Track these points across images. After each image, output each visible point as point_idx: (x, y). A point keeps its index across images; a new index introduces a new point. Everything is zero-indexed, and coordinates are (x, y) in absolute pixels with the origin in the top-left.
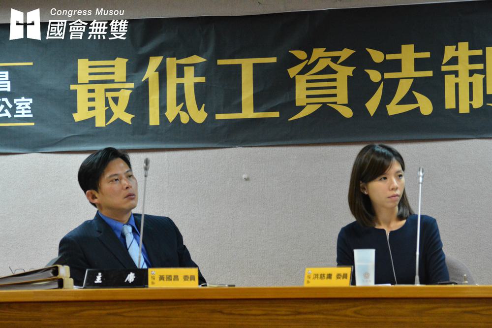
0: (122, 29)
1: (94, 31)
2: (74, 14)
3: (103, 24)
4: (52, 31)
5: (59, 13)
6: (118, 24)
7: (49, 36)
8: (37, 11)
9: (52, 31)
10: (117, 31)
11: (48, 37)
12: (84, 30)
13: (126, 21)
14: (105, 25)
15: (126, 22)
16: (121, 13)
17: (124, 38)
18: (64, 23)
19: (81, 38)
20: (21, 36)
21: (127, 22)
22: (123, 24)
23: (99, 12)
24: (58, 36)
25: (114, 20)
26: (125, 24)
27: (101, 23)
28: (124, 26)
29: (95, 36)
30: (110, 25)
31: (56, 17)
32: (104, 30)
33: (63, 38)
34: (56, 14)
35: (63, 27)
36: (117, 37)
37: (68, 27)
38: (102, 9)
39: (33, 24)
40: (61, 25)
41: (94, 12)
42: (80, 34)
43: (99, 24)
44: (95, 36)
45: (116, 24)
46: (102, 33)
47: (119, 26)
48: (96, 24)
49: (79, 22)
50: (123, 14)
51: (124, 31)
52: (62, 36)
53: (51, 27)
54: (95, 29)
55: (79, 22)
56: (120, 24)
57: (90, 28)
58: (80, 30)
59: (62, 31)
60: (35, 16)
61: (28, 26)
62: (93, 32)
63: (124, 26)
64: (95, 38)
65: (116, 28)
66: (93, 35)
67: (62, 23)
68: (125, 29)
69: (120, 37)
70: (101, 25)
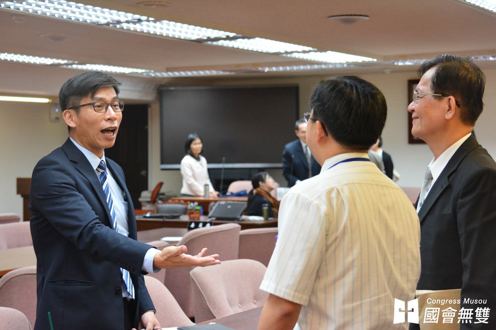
1: (463, 317)
3: (469, 311)
4: (428, 316)
5: (434, 302)
7: (426, 321)
9: (428, 316)
12: (454, 316)
14: (471, 312)
15: (488, 309)
17: (487, 323)
19: (452, 322)
23: (466, 301)
24: (433, 320)
25: (478, 308)
27: (468, 310)
32: (470, 316)
33: (437, 322)
35: (437, 313)
36: (481, 322)
37: (441, 313)
38: (469, 299)
43: (466, 311)
48: (464, 311)
49: (450, 310)
51: (486, 316)
53: (427, 313)
54: (463, 315)
57: (459, 314)
58: (451, 316)
59: (436, 317)
61: (409, 313)
64: (463, 322)
65: (480, 314)
66: (461, 320)
69: (483, 322)
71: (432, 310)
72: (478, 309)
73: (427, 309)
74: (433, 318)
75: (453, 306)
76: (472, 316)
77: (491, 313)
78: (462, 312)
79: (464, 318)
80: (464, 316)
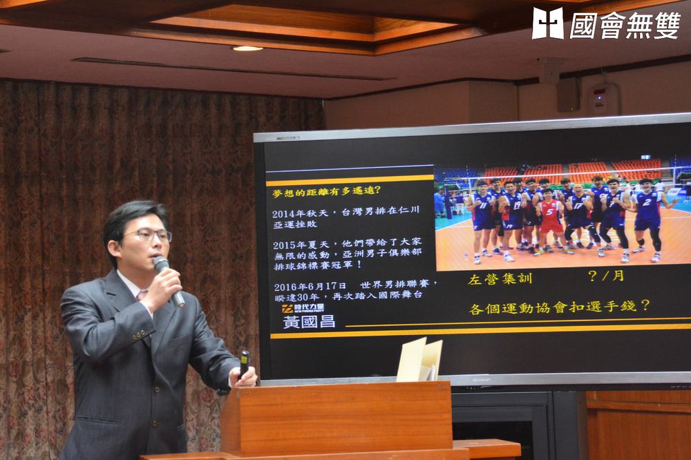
0: (672, 25)
1: (635, 28)
3: (646, 18)
4: (577, 27)
7: (574, 34)
9: (577, 27)
10: (666, 27)
11: (572, 36)
12: (620, 27)
13: (677, 14)
14: (648, 20)
15: (677, 15)
17: (675, 38)
19: (616, 37)
21: (680, 16)
22: (673, 18)
24: (586, 34)
25: (661, 13)
27: (644, 16)
29: (635, 34)
32: (647, 27)
33: (592, 37)
35: (592, 22)
36: (665, 36)
40: (589, 20)
43: (641, 18)
44: (635, 34)
45: (664, 18)
46: (645, 30)
48: (637, 18)
49: (614, 16)
51: (674, 27)
52: (591, 34)
53: (576, 21)
54: (635, 25)
55: (614, 16)
56: (670, 18)
57: (629, 23)
58: (616, 26)
59: (591, 28)
62: (632, 30)
63: (675, 22)
64: (635, 37)
65: (663, 24)
66: (633, 33)
67: (591, 17)
69: (669, 36)
70: (644, 19)
71: (584, 17)
72: (660, 15)
73: (575, 14)
74: (586, 31)
77: (682, 22)
79: (637, 30)
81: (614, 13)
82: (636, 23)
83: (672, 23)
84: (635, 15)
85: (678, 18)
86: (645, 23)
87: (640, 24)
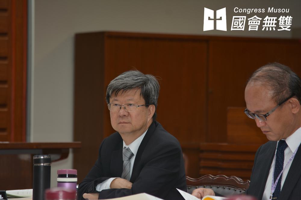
0: (288, 23)
1: (267, 24)
2: (252, 12)
3: (273, 19)
4: (235, 24)
6: (284, 19)
8: (225, 8)
9: (235, 24)
10: (284, 24)
11: (232, 29)
12: (259, 24)
13: (290, 16)
14: (274, 20)
15: (290, 17)
16: (287, 11)
17: (289, 30)
18: (244, 18)
19: (257, 30)
20: (213, 29)
21: (292, 18)
22: (288, 19)
23: (270, 10)
24: (240, 28)
25: (281, 16)
26: (290, 19)
27: (272, 18)
28: (289, 21)
29: (267, 28)
30: (279, 20)
31: (239, 14)
32: (274, 24)
33: (243, 29)
34: (238, 11)
35: (243, 21)
36: (284, 29)
37: (247, 21)
38: (273, 8)
39: (221, 19)
40: (242, 20)
41: (266, 10)
42: (256, 27)
43: (270, 19)
44: (267, 28)
45: (283, 19)
47: (286, 20)
48: (268, 19)
50: (288, 12)
51: (289, 24)
52: (242, 28)
53: (234, 21)
54: (267, 23)
56: (286, 19)
57: (264, 22)
58: (256, 24)
59: (243, 24)
60: (222, 13)
61: (217, 21)
63: (289, 21)
64: (267, 29)
65: (283, 22)
66: (266, 27)
67: (243, 18)
68: (290, 23)
69: (286, 29)
70: (272, 20)
71: (239, 18)
72: (281, 17)
73: (234, 17)
74: (240, 26)
75: (259, 15)
76: (275, 24)
77: (293, 21)
78: (266, 20)
79: (268, 26)
80: (268, 24)
81: (256, 16)
82: (267, 22)
83: (288, 22)
84: (267, 17)
85: (291, 19)
86: (273, 22)
87: (269, 23)
